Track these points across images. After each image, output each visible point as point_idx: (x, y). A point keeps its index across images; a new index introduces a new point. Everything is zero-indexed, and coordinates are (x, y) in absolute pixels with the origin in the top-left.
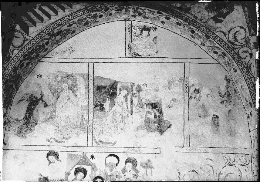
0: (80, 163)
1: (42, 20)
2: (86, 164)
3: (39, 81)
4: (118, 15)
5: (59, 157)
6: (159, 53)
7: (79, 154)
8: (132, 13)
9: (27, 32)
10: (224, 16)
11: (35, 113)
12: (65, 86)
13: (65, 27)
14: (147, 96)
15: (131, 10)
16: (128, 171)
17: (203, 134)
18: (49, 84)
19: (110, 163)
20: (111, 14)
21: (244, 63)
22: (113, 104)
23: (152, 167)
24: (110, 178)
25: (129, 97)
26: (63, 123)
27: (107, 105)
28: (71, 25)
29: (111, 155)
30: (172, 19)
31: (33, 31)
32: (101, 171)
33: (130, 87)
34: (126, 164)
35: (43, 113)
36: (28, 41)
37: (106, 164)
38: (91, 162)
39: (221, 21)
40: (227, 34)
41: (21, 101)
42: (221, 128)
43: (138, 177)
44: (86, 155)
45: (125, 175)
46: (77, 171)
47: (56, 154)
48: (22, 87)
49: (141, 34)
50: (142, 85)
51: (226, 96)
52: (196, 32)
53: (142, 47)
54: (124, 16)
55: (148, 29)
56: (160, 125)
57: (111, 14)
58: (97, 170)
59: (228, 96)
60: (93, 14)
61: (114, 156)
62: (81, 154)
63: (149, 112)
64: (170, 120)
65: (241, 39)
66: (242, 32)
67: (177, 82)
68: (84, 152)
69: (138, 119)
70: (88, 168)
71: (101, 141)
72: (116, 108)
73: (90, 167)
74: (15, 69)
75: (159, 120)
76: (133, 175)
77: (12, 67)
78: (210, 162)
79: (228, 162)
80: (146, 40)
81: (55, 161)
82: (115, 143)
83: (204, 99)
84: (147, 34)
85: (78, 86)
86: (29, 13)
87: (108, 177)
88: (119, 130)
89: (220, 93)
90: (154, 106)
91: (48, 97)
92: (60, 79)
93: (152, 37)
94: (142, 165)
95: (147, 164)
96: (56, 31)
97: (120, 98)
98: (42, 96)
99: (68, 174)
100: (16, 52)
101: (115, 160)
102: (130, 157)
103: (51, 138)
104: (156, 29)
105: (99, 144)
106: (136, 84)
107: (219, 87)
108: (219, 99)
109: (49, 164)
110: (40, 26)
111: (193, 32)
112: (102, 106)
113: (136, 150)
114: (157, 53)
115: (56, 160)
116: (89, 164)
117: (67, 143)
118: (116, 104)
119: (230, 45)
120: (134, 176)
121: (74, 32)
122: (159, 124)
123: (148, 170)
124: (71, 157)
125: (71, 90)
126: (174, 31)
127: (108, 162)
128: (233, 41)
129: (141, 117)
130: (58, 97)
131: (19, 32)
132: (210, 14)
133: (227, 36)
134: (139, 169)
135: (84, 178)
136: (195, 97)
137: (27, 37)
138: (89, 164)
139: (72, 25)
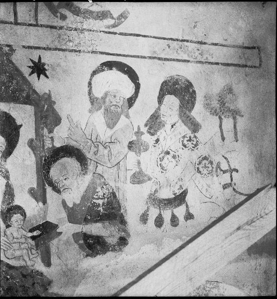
2: (13, 98)
16: (168, 126)
19: (106, 94)
24: (106, 151)
29: (109, 65)
37: (93, 100)
43: (196, 145)
45: (157, 141)
58: (57, 121)
70: (24, 115)
73: (29, 109)
76: (184, 137)
87: (101, 147)
101: (120, 84)
102: (174, 73)
113: (190, 49)
116: (28, 96)
120: (185, 142)
123: (225, 121)
135: (8, 152)
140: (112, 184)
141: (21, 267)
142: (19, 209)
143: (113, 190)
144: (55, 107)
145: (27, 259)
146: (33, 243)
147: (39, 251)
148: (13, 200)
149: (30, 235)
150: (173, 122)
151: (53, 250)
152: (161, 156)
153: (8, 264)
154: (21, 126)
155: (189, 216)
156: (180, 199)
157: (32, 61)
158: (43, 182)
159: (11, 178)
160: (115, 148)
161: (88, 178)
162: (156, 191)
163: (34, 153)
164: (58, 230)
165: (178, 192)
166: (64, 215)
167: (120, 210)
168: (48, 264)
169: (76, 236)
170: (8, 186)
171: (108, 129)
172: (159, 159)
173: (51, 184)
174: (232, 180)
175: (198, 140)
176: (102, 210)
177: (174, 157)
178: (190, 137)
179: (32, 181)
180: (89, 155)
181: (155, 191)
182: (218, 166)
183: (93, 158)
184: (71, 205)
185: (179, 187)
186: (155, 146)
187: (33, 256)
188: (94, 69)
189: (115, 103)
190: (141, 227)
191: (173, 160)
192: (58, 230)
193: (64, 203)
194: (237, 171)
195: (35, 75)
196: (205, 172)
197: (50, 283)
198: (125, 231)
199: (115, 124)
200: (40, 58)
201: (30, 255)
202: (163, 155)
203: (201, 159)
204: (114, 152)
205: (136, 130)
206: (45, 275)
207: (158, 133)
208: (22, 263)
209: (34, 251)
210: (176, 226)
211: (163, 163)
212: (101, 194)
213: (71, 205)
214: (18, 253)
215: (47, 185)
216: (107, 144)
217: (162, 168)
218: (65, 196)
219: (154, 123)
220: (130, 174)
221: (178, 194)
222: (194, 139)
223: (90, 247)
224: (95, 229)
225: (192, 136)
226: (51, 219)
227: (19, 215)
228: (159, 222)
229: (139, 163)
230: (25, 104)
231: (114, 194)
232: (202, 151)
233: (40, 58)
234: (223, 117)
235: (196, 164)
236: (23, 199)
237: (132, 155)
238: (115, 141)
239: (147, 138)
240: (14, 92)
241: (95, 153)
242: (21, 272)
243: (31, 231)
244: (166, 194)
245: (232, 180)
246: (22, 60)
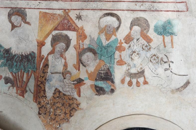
0: (59, 28)
2: (69, 29)
7: (58, 12)
16: (135, 40)
19: (106, 26)
23: (172, 34)
24: (106, 50)
29: (108, 14)
32: (92, 40)
34: (131, 29)
38: (77, 26)
43: (150, 49)
44: (70, 14)
45: (130, 46)
46: (55, 40)
58: (85, 37)
68: (65, 10)
70: (72, 35)
76: (143, 45)
81: (21, 25)
87: (103, 49)
94: (156, 29)
99: (41, 44)
102: (138, 16)
109: (12, 29)
115: (22, 22)
120: (144, 47)
127: (103, 25)
135: (67, 50)
138: (74, 28)
140: (108, 65)
141: (69, 95)
142: (69, 72)
143: (108, 67)
144: (85, 32)
145: (71, 92)
146: (73, 86)
147: (76, 90)
148: (67, 68)
149: (73, 83)
150: (138, 38)
152: (131, 53)
153: (64, 93)
154: (71, 39)
155: (146, 83)
156: (141, 73)
157: (76, 14)
158: (79, 62)
159: (67, 60)
160: (110, 49)
161: (98, 61)
162: (129, 69)
163: (76, 50)
164: (84, 82)
165: (140, 70)
167: (111, 76)
168: (80, 96)
169: (91, 86)
170: (65, 62)
171: (107, 41)
172: (130, 55)
174: (170, 67)
175: (150, 46)
176: (103, 76)
177: (138, 54)
178: (146, 45)
179: (75, 61)
180: (98, 52)
181: (128, 69)
182: (162, 59)
183: (100, 53)
184: (89, 72)
185: (140, 68)
186: (128, 49)
187: (73, 92)
188: (100, 16)
189: (110, 30)
190: (121, 85)
191: (137, 55)
192: (84, 82)
193: (87, 71)
194: (173, 63)
195: (77, 20)
196: (154, 62)
197: (79, 104)
198: (114, 86)
199: (110, 39)
200: (79, 13)
201: (72, 91)
202: (132, 53)
203: (152, 55)
204: (109, 51)
205: (119, 41)
206: (78, 100)
207: (130, 43)
208: (69, 94)
209: (74, 90)
210: (139, 86)
211: (132, 57)
212: (103, 69)
213: (89, 72)
214: (68, 89)
215: (80, 63)
216: (106, 47)
217: (132, 59)
218: (87, 68)
219: (128, 39)
220: (116, 61)
221: (140, 72)
222: (148, 46)
223: (97, 91)
224: (101, 84)
225: (148, 44)
226: (82, 77)
227: (69, 74)
228: (130, 84)
229: (120, 56)
230: (73, 31)
231: (108, 69)
232: (153, 52)
233: (79, 13)
234: (165, 36)
235: (150, 58)
236: (70, 68)
237: (117, 53)
238: (110, 46)
239: (124, 45)
240: (69, 26)
241: (101, 51)
242: (69, 98)
243: (74, 81)
244: (133, 71)
245: (170, 67)
246: (73, 15)
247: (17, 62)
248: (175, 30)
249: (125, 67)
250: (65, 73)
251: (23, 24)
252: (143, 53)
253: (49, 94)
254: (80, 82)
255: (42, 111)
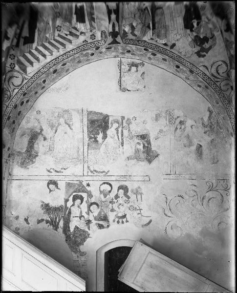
1: (38, 59)
2: (83, 192)
3: (38, 117)
4: (108, 53)
5: (58, 186)
6: (146, 87)
7: (76, 182)
8: (121, 51)
9: (26, 72)
10: (207, 51)
11: (36, 146)
12: (62, 120)
13: (59, 67)
14: (136, 128)
15: (119, 48)
17: (188, 162)
18: (47, 119)
20: (101, 53)
21: (225, 95)
22: (105, 137)
23: (141, 194)
25: (120, 130)
26: (61, 155)
27: (100, 137)
28: (64, 65)
29: (104, 183)
30: (159, 56)
31: (31, 70)
33: (121, 120)
35: (43, 146)
36: (26, 81)
37: (100, 191)
39: (204, 56)
40: (209, 68)
41: (23, 135)
42: (204, 156)
46: (74, 200)
47: (55, 183)
48: (24, 122)
49: (130, 70)
50: (131, 119)
51: (209, 126)
52: (181, 67)
53: (131, 82)
54: (114, 54)
55: (136, 66)
56: (149, 155)
57: (101, 53)
59: (211, 127)
60: (84, 53)
61: (107, 183)
62: (78, 182)
63: (138, 143)
64: (157, 150)
65: (223, 73)
66: (224, 66)
67: (164, 115)
69: (130, 148)
70: (84, 195)
71: (95, 171)
72: (108, 139)
74: (16, 107)
75: (147, 150)
77: (13, 105)
78: (194, 188)
79: (211, 187)
80: (134, 76)
82: (108, 172)
83: (188, 129)
84: (136, 70)
85: (73, 120)
86: (25, 54)
88: (112, 160)
89: (203, 124)
90: (143, 137)
91: (48, 132)
92: (57, 114)
93: (140, 73)
94: (132, 191)
95: (137, 191)
96: (52, 70)
97: (111, 132)
98: (42, 130)
99: (67, 201)
100: (16, 91)
103: (51, 169)
104: (143, 65)
105: (94, 174)
106: (126, 118)
107: (202, 119)
108: (201, 130)
110: (37, 66)
111: (178, 67)
112: (95, 138)
114: (145, 87)
117: (65, 172)
118: (108, 136)
119: (212, 78)
121: (68, 70)
122: (147, 154)
124: (69, 185)
125: (67, 124)
126: (160, 66)
127: (102, 190)
128: (216, 74)
129: (131, 148)
130: (56, 131)
131: (19, 72)
132: (194, 49)
133: (209, 70)
134: (130, 196)
136: (180, 128)
137: (24, 75)
139: (66, 64)
151: (90, 226)
156: (125, 216)
166: (93, 218)
169: (96, 224)
170: (81, 211)
173: (90, 211)
190: (113, 223)
218: (94, 214)
219: (117, 197)
224: (101, 223)
232: (131, 204)
236: (84, 214)
239: (115, 201)
244: (120, 215)
246: (85, 184)
247: (53, 211)
248: (143, 191)
249: (115, 213)
250: (81, 217)
251: (56, 189)
252: (125, 205)
253: (72, 230)
254: (89, 222)
255: (68, 238)
